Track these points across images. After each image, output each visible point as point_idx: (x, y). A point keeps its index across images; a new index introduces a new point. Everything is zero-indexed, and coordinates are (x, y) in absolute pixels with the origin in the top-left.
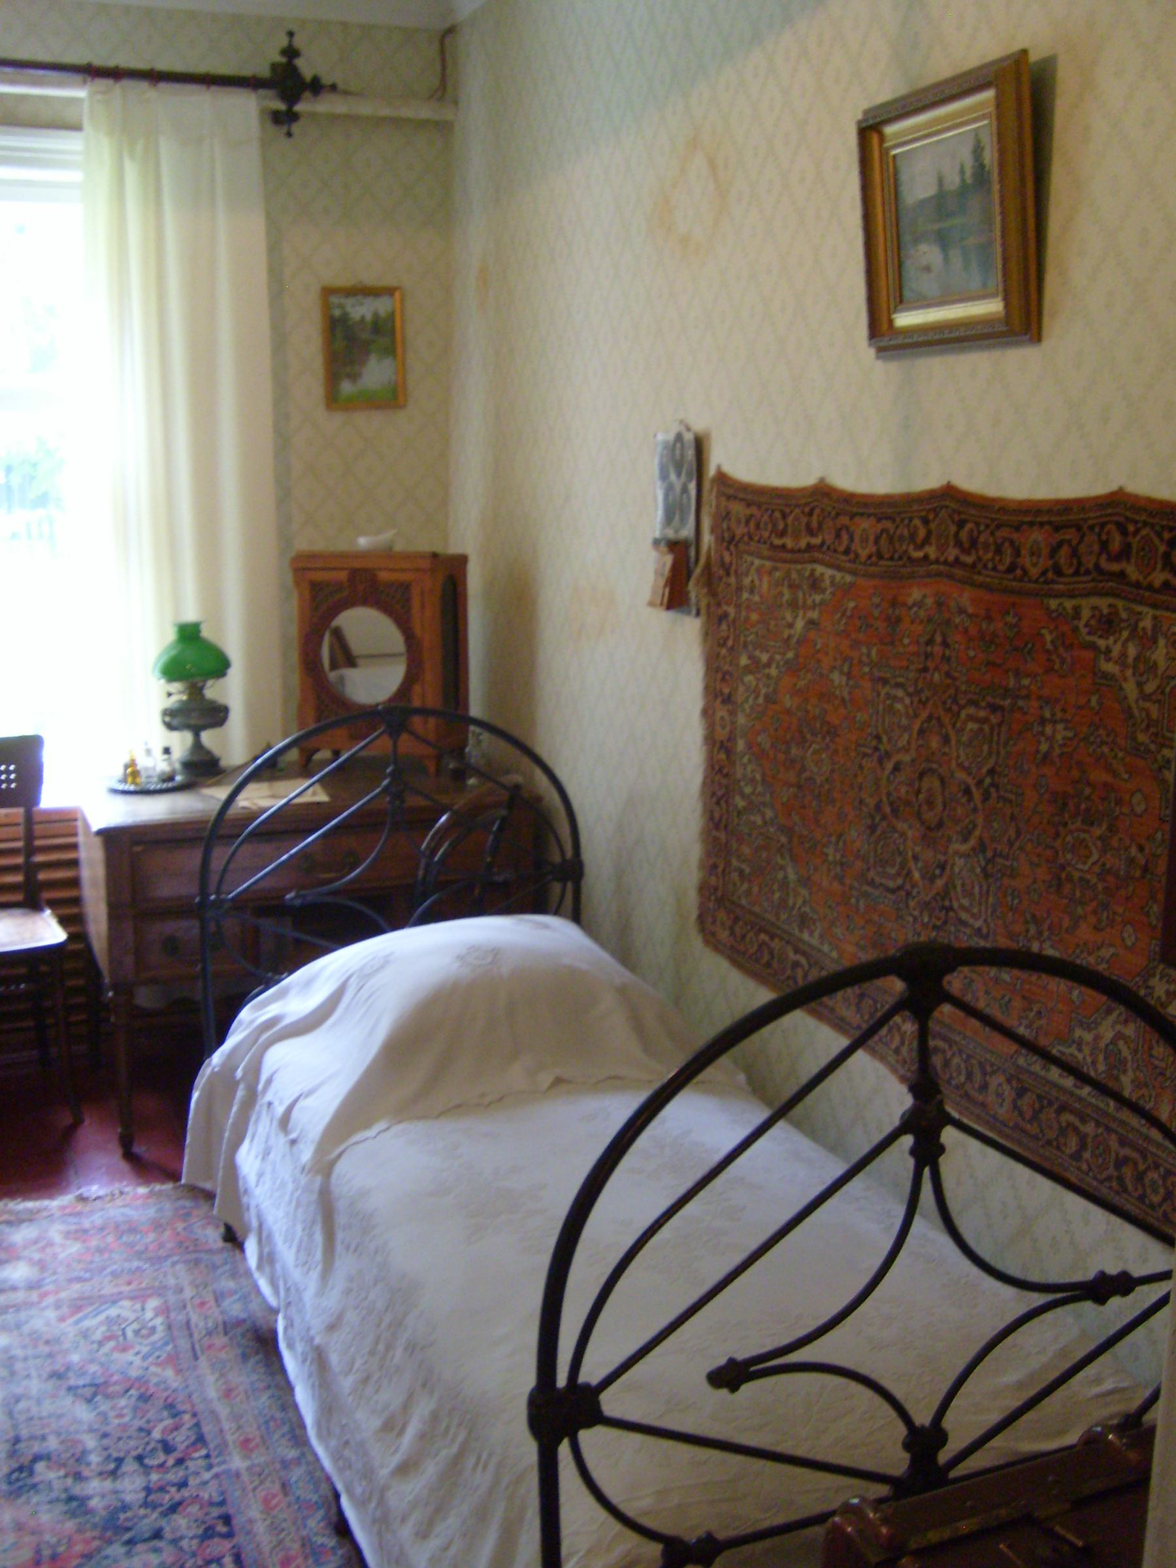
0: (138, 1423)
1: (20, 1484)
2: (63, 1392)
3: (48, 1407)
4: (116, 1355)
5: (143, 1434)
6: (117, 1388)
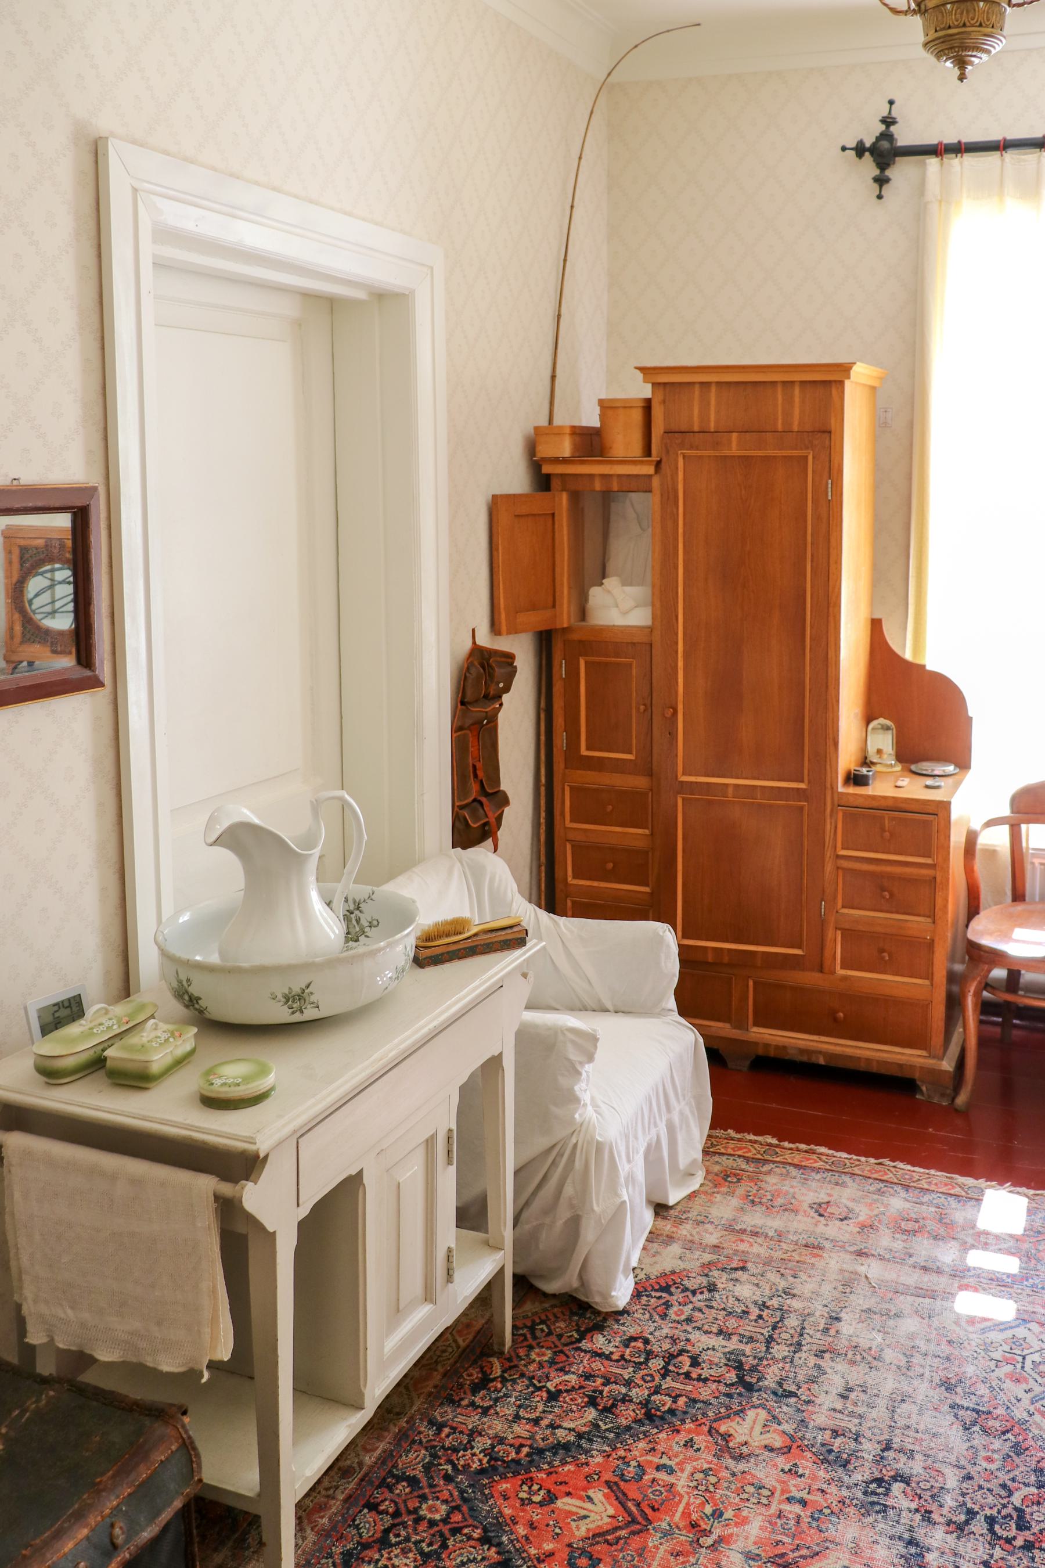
0: (1003, 1477)
1: (875, 1499)
2: (945, 1408)
3: (927, 1420)
4: (1008, 1384)
5: (1003, 1493)
6: (996, 1424)
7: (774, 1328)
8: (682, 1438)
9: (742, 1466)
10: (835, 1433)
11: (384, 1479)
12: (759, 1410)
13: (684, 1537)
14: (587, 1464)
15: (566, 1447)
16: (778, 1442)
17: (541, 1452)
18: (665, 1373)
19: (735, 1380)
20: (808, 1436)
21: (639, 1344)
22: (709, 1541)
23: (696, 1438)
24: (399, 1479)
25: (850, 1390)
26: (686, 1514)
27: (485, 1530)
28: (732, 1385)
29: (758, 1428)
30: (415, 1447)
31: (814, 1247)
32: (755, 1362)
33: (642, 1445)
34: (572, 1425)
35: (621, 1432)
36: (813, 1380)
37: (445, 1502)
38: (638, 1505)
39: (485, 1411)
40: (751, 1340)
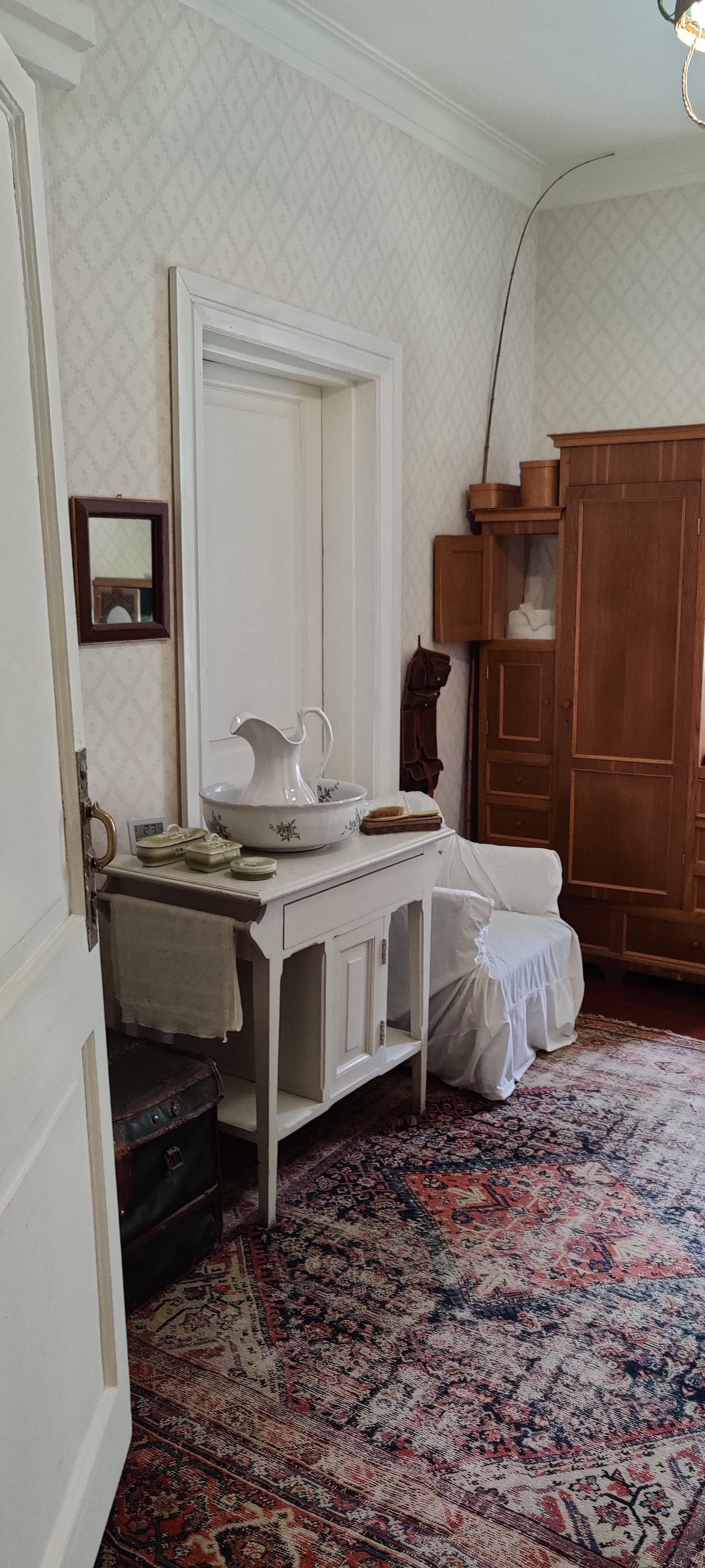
1: (672, 1217)
7: (615, 1123)
8: (538, 1170)
9: (579, 1188)
10: (650, 1181)
11: (336, 1164)
12: (596, 1163)
13: (532, 1216)
14: (471, 1174)
15: (458, 1165)
16: (607, 1180)
17: (440, 1165)
18: (531, 1137)
19: (581, 1146)
20: (629, 1180)
21: (516, 1121)
22: (549, 1220)
23: (547, 1171)
24: (344, 1165)
25: (666, 1162)
26: (535, 1205)
27: (399, 1195)
28: (579, 1149)
29: (594, 1171)
30: (356, 1152)
31: (654, 1086)
32: (597, 1140)
33: (509, 1170)
34: (462, 1155)
35: (495, 1163)
36: (637, 1153)
37: (375, 1179)
38: (503, 1197)
39: (404, 1141)
40: (596, 1128)
